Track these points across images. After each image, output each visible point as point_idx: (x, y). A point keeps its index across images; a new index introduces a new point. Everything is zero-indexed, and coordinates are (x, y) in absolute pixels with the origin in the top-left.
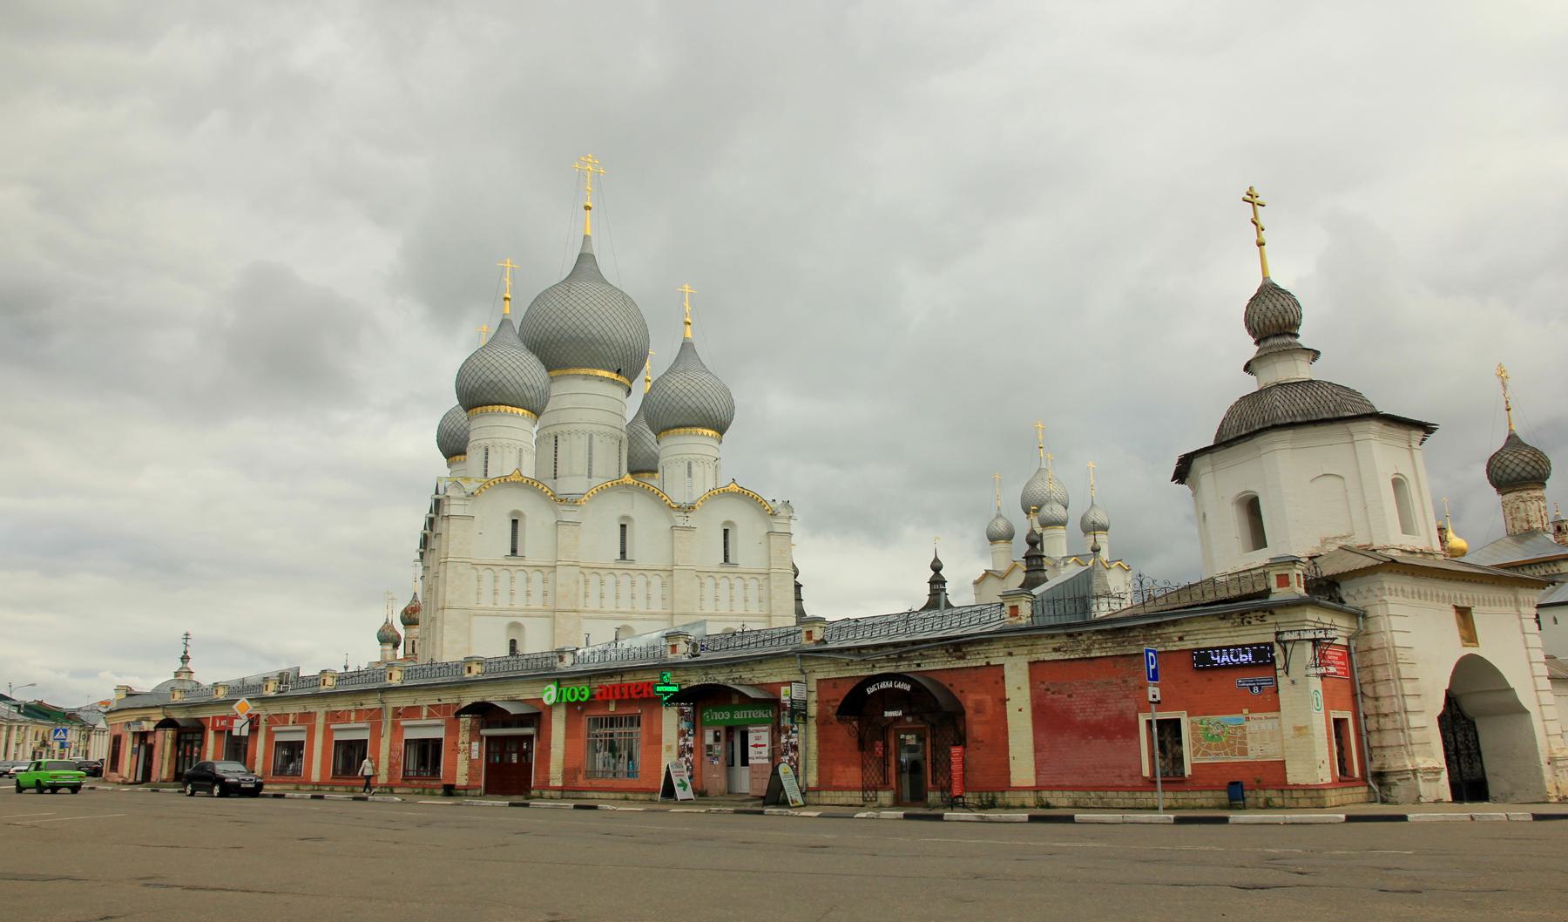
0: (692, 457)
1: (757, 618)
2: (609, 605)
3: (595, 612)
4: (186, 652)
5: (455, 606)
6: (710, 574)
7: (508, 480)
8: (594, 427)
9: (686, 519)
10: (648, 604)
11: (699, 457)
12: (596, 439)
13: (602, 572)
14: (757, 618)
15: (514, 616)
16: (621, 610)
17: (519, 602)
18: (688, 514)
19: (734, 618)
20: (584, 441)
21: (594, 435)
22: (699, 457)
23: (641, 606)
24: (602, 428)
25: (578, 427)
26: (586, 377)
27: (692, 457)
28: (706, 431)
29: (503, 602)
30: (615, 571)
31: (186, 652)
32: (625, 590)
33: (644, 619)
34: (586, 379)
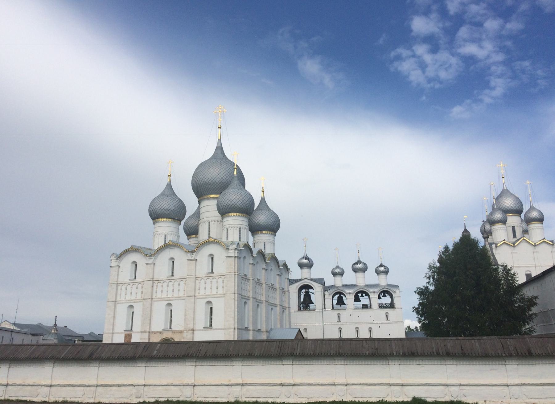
0: (228, 226)
1: (220, 296)
2: (164, 295)
3: (158, 298)
4: (55, 323)
5: (110, 301)
6: (202, 278)
7: (129, 250)
8: (210, 219)
9: (192, 256)
10: (179, 293)
11: (230, 226)
12: (211, 224)
13: (162, 282)
14: (220, 296)
15: (131, 302)
16: (168, 296)
17: (133, 297)
18: (193, 254)
19: (211, 296)
20: (207, 224)
21: (210, 222)
22: (230, 226)
23: (176, 295)
24: (213, 219)
25: (205, 219)
26: (208, 199)
27: (228, 226)
28: (233, 214)
29: (128, 298)
30: (167, 281)
31: (55, 323)
32: (171, 289)
33: (176, 300)
34: (208, 200)
